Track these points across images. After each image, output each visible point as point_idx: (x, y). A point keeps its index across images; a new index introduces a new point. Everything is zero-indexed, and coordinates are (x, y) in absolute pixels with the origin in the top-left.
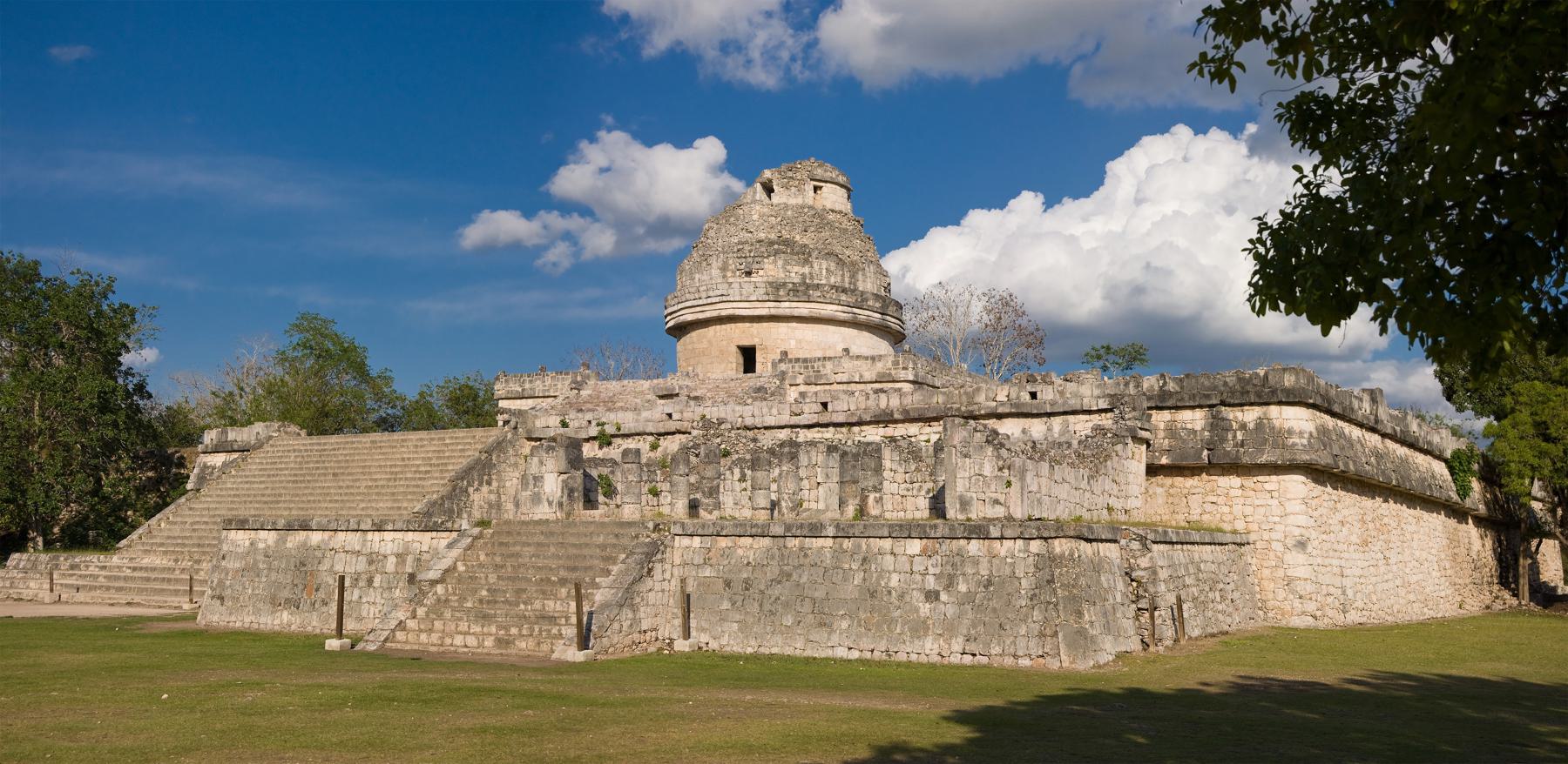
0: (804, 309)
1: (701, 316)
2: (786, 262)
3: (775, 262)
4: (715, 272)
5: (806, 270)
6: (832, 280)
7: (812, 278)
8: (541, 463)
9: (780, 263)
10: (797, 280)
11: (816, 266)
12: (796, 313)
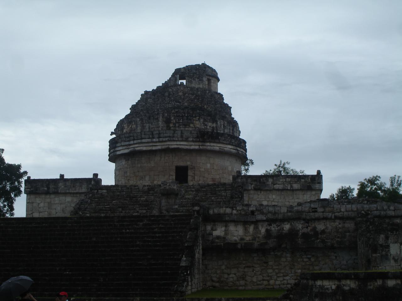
1: (154, 148)
2: (205, 120)
5: (214, 125)
6: (226, 131)
7: (217, 130)
8: (387, 238)
9: (202, 120)
10: (210, 130)
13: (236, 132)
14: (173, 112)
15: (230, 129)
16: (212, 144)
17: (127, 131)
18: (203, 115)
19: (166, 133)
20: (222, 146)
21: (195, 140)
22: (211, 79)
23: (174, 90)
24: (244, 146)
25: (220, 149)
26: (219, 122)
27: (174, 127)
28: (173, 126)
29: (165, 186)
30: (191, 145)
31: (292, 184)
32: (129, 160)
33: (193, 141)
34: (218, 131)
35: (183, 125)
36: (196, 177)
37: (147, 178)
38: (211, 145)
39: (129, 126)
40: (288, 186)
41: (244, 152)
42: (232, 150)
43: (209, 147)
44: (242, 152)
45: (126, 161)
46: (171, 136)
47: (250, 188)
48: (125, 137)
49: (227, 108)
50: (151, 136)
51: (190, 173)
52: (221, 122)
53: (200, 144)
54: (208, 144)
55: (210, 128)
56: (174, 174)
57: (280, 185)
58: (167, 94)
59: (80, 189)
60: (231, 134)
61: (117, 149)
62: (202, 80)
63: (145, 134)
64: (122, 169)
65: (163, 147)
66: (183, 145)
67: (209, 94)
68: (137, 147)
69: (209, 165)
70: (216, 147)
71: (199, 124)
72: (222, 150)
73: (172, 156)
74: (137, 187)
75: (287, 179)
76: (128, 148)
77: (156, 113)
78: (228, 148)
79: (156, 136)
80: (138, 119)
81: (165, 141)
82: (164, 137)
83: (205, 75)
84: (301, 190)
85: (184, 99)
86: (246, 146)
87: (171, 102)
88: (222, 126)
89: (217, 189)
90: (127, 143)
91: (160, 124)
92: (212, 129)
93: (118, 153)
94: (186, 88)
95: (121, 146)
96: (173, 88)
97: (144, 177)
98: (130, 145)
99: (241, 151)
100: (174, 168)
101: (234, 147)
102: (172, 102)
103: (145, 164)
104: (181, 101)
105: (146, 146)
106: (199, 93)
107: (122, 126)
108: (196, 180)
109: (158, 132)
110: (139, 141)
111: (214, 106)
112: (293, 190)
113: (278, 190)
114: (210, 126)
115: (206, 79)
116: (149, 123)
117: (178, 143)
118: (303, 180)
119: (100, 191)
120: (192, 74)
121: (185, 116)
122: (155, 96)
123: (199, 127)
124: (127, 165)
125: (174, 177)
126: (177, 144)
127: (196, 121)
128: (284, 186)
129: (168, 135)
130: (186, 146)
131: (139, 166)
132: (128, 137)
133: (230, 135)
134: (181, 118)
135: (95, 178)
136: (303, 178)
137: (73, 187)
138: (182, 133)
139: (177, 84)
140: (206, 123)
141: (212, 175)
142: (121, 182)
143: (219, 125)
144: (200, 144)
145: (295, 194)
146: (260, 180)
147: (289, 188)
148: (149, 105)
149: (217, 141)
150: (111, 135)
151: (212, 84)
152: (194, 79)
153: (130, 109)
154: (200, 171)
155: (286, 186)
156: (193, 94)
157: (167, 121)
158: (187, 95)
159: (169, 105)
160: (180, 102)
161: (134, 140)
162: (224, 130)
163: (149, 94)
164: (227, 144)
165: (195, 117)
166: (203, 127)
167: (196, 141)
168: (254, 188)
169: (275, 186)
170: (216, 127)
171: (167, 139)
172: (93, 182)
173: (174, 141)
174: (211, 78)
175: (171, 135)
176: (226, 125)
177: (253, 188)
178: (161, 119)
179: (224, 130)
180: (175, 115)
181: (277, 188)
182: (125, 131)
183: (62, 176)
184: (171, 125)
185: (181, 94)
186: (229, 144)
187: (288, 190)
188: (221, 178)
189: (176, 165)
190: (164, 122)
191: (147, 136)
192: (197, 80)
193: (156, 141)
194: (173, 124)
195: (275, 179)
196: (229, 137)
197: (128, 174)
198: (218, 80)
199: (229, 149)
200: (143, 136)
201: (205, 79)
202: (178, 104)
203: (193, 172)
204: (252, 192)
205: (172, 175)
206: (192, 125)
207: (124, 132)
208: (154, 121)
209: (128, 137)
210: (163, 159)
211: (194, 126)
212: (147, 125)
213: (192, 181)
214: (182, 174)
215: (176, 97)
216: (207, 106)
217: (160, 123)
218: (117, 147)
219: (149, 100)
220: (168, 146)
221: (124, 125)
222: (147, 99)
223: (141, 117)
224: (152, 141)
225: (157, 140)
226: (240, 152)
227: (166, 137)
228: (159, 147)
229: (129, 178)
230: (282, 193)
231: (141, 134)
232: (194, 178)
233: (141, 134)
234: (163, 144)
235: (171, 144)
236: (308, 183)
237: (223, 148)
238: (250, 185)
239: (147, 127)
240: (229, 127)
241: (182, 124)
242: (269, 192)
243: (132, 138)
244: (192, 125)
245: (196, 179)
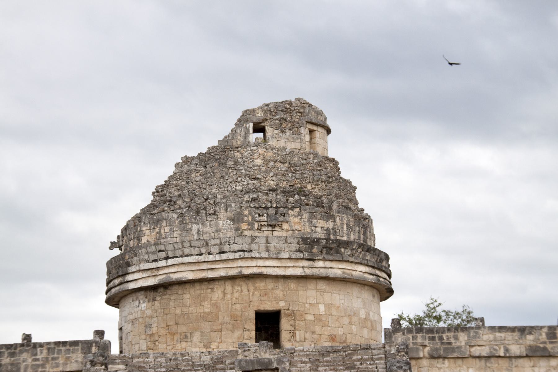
0: (337, 269)
1: (210, 275)
2: (312, 216)
3: (300, 214)
4: (224, 223)
5: (330, 225)
6: (352, 237)
7: (335, 234)
9: (306, 216)
10: (322, 236)
11: (338, 219)
12: (331, 273)
13: (370, 239)
14: (245, 199)
15: (359, 233)
16: (328, 264)
17: (150, 240)
18: (307, 204)
19: (234, 243)
20: (348, 268)
21: (294, 256)
22: (315, 131)
23: (245, 154)
24: (387, 266)
25: (344, 273)
26: (338, 218)
27: (250, 230)
28: (247, 229)
29: (246, 353)
30: (285, 267)
31: (508, 345)
32: (154, 300)
33: (290, 258)
34: (338, 238)
35: (268, 225)
36: (297, 333)
37: (197, 337)
39: (154, 229)
40: (500, 348)
41: (388, 278)
42: (367, 276)
43: (322, 270)
44: (385, 279)
45: (149, 302)
46: (244, 249)
47: (421, 355)
48: (147, 253)
49: (348, 189)
50: (203, 250)
51: (285, 324)
52: (342, 217)
53: (306, 263)
54: (321, 264)
55: (322, 232)
56: (254, 327)
57: (483, 347)
58: (230, 163)
59: (66, 364)
60: (362, 242)
61: (129, 278)
62: (299, 134)
63: (191, 246)
64: (140, 320)
65: (233, 272)
66: (272, 267)
67: (315, 161)
68: (175, 272)
69: (322, 308)
70: (337, 269)
71: (300, 223)
72: (348, 275)
73: (248, 291)
74: (187, 357)
75: (498, 334)
77: (212, 202)
78: (360, 271)
79: (216, 249)
80: (175, 216)
81: (233, 260)
82: (229, 252)
83: (305, 123)
84: (527, 356)
85: (266, 172)
86: (389, 266)
87: (239, 180)
88: (345, 226)
89: (354, 358)
90: (154, 265)
91: (221, 225)
92: (325, 232)
93: (132, 286)
94: (270, 150)
95: (140, 271)
96: (242, 151)
97: (189, 335)
98: (158, 269)
99: (383, 278)
100: (254, 316)
101: (371, 269)
102: (243, 180)
103: (191, 309)
104: (260, 177)
106: (296, 159)
107: (139, 228)
108: (298, 340)
109: (218, 241)
110: (180, 260)
111: (326, 186)
112: (510, 357)
113: (479, 357)
114: (322, 228)
115: (307, 130)
116: (197, 223)
117: (261, 263)
118: (530, 338)
119: (112, 368)
120: (278, 121)
121: (271, 207)
122: (205, 167)
123: (300, 229)
124: (152, 311)
125: (253, 334)
126: (258, 265)
127: (295, 216)
128: (492, 350)
129: (239, 247)
130: (276, 269)
131: (178, 311)
132: (153, 253)
133: (362, 244)
134: (265, 211)
135: (98, 339)
136: (530, 333)
137: (53, 359)
138: (267, 241)
139: (249, 142)
140: (314, 221)
141: (329, 328)
142: (137, 346)
143: (339, 224)
144: (305, 265)
145: (516, 366)
146: (441, 338)
147: (502, 354)
148: (194, 186)
149: (338, 257)
150: (111, 248)
151: (317, 140)
152: (282, 131)
153: (153, 193)
154: (305, 320)
155: (495, 350)
156: (283, 161)
157: (237, 219)
158: (272, 163)
159: (236, 186)
160: (258, 179)
161: (167, 258)
162: (348, 235)
163: (194, 162)
164: (356, 263)
165: (292, 208)
166: (309, 230)
167: (297, 259)
168: (429, 354)
169: (473, 349)
170: (334, 229)
171: (237, 255)
172: (94, 349)
173: (252, 258)
174: (314, 128)
175: (246, 247)
176: (352, 224)
177: (427, 355)
178: (222, 213)
179: (348, 235)
180: (252, 205)
181: (477, 354)
182: (144, 240)
183: (27, 338)
184: (244, 226)
185: (259, 162)
186: (361, 264)
187: (499, 357)
190: (230, 220)
191: (196, 251)
192: (288, 133)
193: (214, 260)
194: (249, 225)
195: (472, 334)
196: (360, 250)
197: (154, 330)
198: (329, 131)
199: (361, 273)
200: (187, 251)
201: (304, 131)
202: (255, 182)
203: (292, 322)
204: (425, 362)
205: (249, 330)
206: (285, 226)
207: (143, 242)
208: (209, 219)
209: (153, 253)
210: (229, 296)
211: (291, 226)
212: (195, 227)
213: (290, 341)
214: (268, 325)
215: (251, 168)
216: (313, 186)
217: (221, 223)
218: (128, 274)
219: (193, 175)
220: (239, 269)
221: (144, 229)
222: (189, 172)
223: (178, 211)
224: (206, 260)
225: (218, 257)
226: (381, 279)
227: (235, 252)
228: (222, 273)
229: (156, 339)
230: (488, 365)
231: (183, 247)
232: (294, 335)
233: (183, 247)
234: (230, 264)
235: (247, 265)
236: (541, 343)
237: (351, 271)
238: (421, 348)
239: (194, 231)
240: (358, 229)
241: (266, 223)
242: (460, 362)
243: (163, 255)
244: (285, 226)
245: (298, 337)
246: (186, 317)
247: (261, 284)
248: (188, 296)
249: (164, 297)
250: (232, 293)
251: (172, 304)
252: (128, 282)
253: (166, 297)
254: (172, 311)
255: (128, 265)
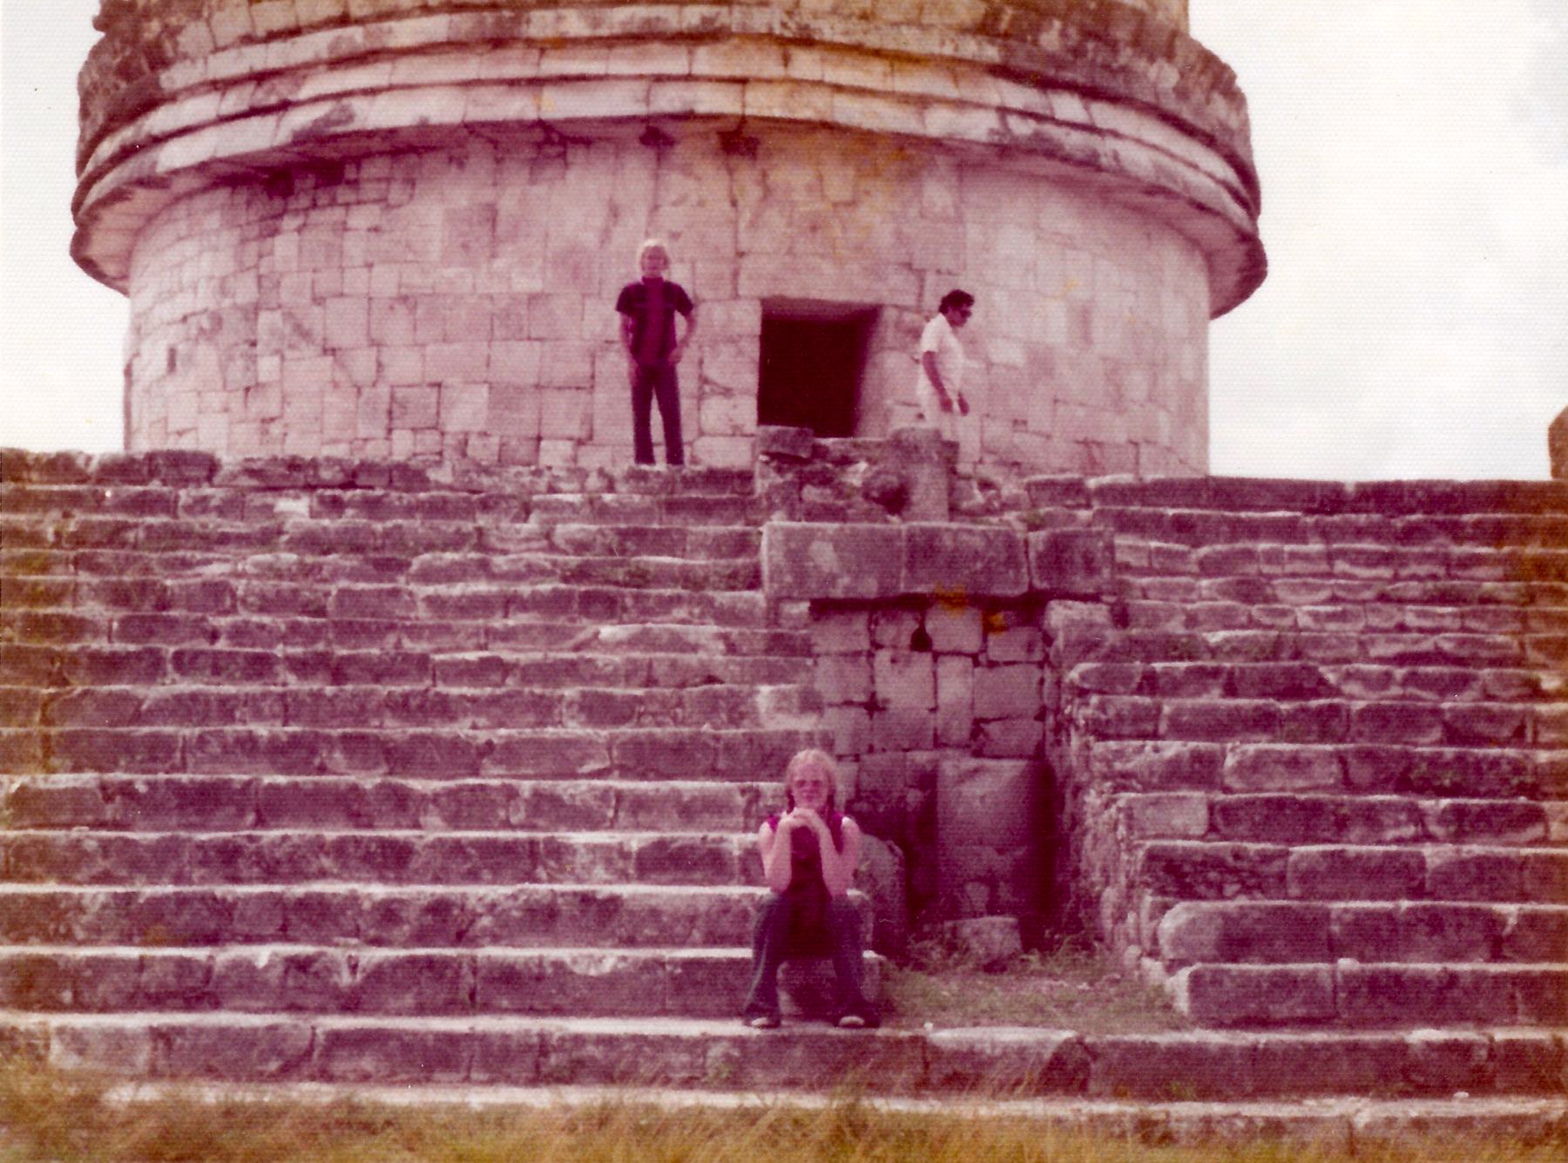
1: (558, 106)
30: (923, 102)
38: (1100, 124)
56: (751, 380)
61: (160, 120)
70: (1139, 145)
76: (284, 106)
78: (1205, 171)
93: (174, 156)
100: (749, 320)
105: (467, 84)
131: (385, 281)
186: (1210, 141)
188: (1136, 444)
189: (766, 289)
229: (273, 410)
246: (420, 311)
247: (792, 176)
248: (435, 211)
249: (315, 216)
250: (655, 208)
251: (355, 246)
252: (158, 140)
253: (337, 214)
254: (357, 281)
255: (160, 62)
